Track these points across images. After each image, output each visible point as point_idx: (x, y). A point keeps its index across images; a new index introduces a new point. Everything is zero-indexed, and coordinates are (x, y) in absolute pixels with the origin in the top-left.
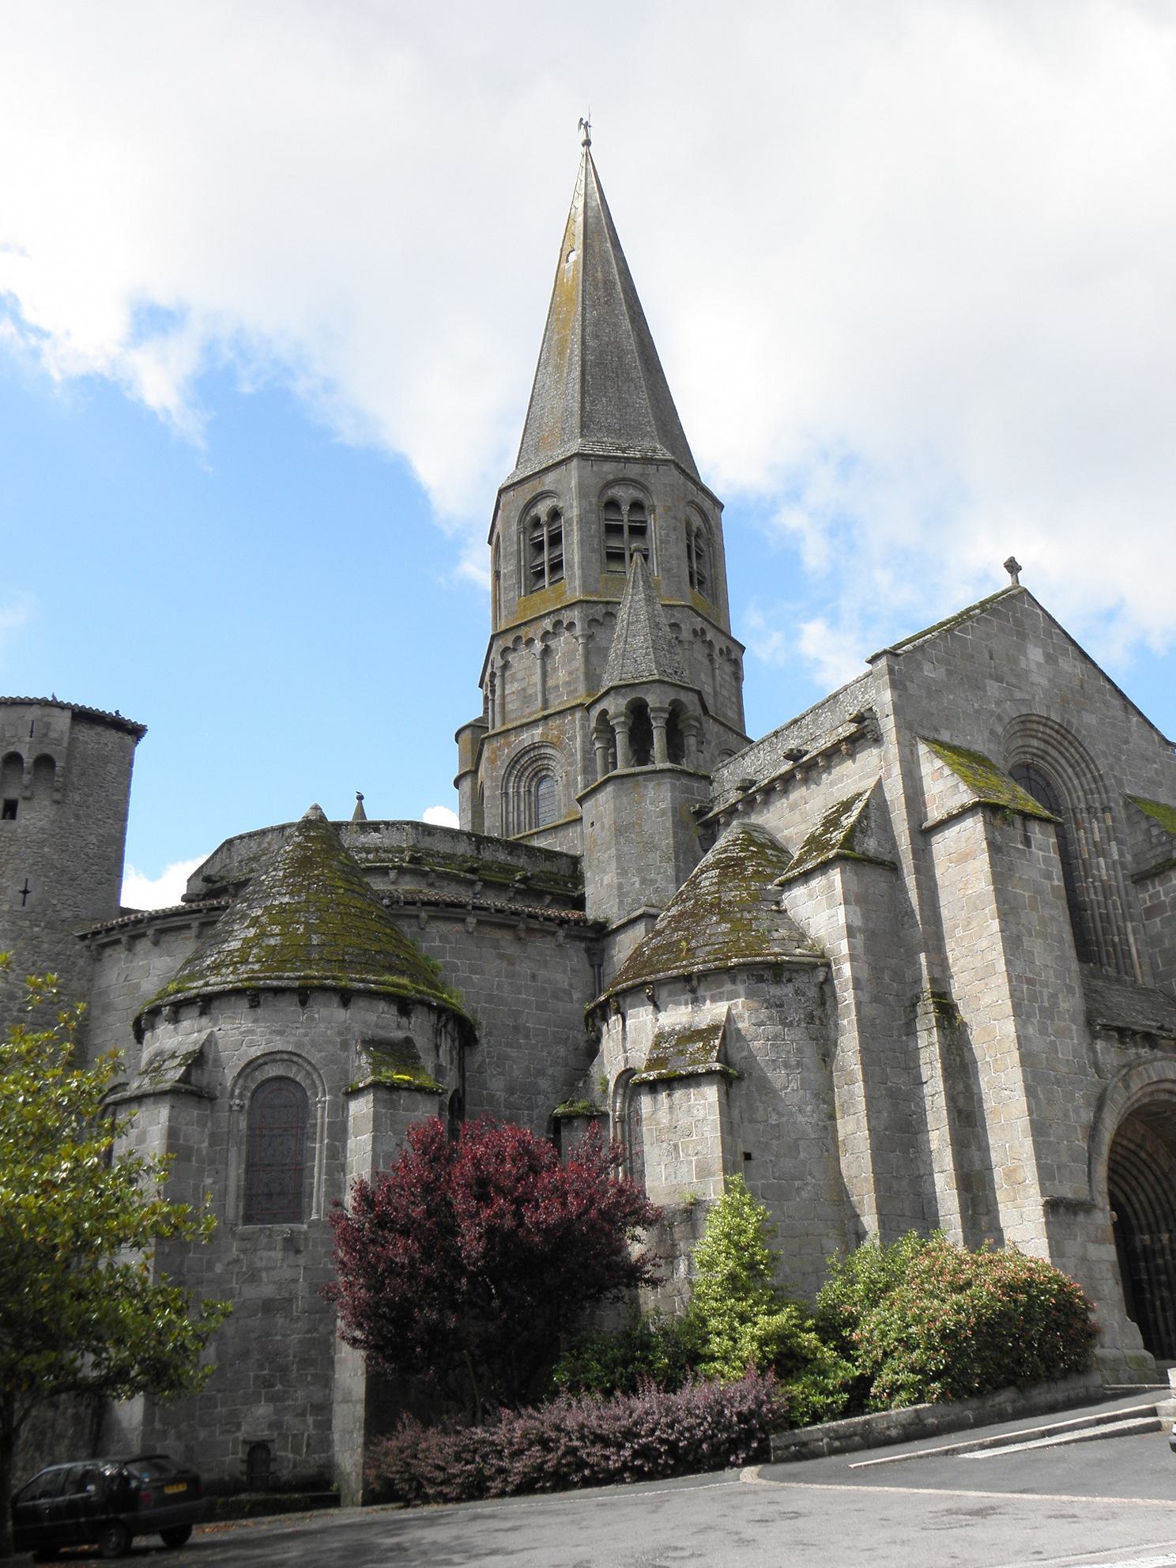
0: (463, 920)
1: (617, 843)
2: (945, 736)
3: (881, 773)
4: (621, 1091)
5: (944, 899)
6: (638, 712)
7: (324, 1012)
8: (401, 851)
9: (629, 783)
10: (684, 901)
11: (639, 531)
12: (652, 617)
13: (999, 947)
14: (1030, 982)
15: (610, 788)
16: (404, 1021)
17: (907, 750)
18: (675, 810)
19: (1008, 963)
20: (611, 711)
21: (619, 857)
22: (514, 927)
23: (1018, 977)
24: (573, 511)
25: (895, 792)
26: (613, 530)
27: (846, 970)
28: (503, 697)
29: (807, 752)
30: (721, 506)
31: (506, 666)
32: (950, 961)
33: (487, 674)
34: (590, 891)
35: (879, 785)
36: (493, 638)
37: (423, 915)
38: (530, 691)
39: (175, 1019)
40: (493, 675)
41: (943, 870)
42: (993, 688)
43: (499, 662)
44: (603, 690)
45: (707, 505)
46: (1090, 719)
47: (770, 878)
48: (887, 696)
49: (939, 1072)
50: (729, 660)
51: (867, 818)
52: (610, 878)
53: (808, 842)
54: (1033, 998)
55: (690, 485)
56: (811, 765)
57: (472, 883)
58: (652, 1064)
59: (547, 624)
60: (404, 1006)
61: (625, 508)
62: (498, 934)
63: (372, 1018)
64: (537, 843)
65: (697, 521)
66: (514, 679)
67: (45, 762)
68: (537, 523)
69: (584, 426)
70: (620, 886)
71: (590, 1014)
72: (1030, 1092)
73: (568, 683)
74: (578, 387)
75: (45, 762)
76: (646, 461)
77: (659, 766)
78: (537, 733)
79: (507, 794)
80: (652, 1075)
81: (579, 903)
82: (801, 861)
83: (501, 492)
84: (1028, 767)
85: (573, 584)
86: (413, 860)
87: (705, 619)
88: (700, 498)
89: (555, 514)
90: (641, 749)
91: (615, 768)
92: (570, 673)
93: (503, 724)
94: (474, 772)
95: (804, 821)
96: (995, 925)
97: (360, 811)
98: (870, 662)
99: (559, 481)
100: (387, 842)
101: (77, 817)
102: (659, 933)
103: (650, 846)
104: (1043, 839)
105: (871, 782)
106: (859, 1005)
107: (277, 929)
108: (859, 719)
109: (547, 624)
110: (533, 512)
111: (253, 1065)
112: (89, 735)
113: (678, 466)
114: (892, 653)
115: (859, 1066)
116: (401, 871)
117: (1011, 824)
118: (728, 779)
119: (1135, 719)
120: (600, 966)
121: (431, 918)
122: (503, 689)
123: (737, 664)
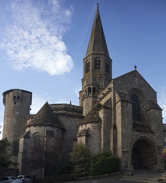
0: (65, 116)
7: (42, 127)
8: (63, 107)
9: (87, 98)
11: (99, 64)
12: (93, 76)
14: (125, 124)
16: (53, 129)
18: (92, 102)
19: (121, 121)
22: (72, 117)
23: (123, 123)
24: (91, 62)
26: (96, 64)
27: (103, 122)
30: (111, 60)
35: (111, 98)
41: (117, 109)
42: (129, 84)
45: (109, 61)
54: (125, 126)
55: (107, 58)
57: (72, 111)
59: (87, 77)
61: (98, 61)
62: (70, 118)
63: (48, 128)
69: (93, 50)
72: (122, 138)
76: (101, 54)
83: (83, 60)
88: (109, 60)
89: (89, 63)
96: (121, 116)
97: (71, 103)
100: (62, 106)
101: (23, 104)
103: (89, 106)
106: (104, 127)
109: (87, 77)
111: (34, 134)
113: (105, 55)
117: (125, 103)
119: (151, 89)
121: (61, 116)
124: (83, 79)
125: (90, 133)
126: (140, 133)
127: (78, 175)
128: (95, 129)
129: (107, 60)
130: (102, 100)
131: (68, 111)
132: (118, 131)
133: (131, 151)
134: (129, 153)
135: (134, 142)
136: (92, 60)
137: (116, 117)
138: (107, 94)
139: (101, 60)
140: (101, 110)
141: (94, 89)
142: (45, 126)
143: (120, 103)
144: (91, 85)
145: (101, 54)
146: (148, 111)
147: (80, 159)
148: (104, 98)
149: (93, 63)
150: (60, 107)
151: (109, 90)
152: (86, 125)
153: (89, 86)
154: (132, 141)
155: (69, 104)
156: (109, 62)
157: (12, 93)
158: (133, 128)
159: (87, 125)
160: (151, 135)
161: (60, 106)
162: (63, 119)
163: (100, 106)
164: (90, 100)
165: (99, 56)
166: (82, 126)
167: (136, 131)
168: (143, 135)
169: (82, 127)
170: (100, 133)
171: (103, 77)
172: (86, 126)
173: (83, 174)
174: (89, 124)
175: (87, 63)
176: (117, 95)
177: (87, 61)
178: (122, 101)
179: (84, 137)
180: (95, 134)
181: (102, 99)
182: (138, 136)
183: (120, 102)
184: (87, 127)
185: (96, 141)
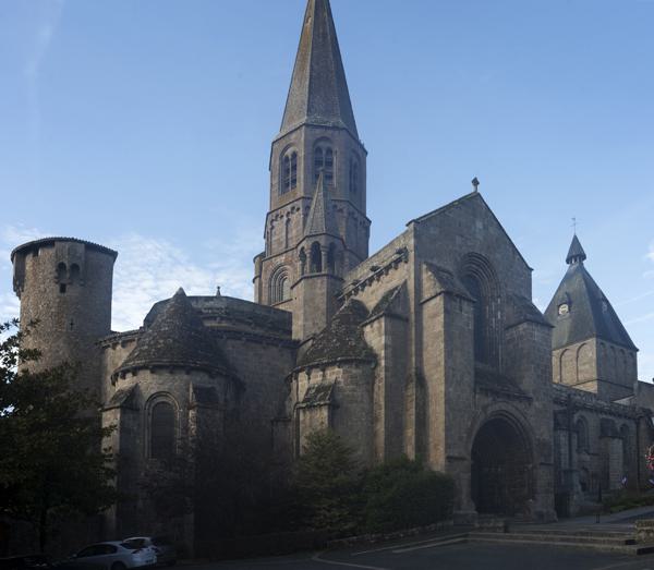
0: (240, 339)
2: (435, 262)
5: (425, 334)
6: (316, 246)
9: (310, 281)
11: (330, 164)
12: (325, 204)
13: (443, 355)
14: (453, 369)
22: (261, 343)
24: (301, 154)
26: (318, 163)
27: (383, 363)
31: (272, 228)
34: (294, 328)
35: (405, 282)
39: (124, 377)
41: (426, 322)
42: (458, 240)
45: (360, 152)
46: (498, 256)
47: (358, 324)
52: (301, 322)
54: (454, 376)
57: (250, 324)
58: (305, 401)
59: (289, 208)
61: (324, 152)
62: (253, 345)
65: (355, 160)
67: (75, 267)
71: (286, 379)
72: (447, 414)
75: (75, 267)
76: (335, 128)
77: (323, 272)
80: (304, 405)
81: (290, 332)
83: (274, 143)
84: (470, 276)
89: (295, 155)
96: (442, 346)
99: (296, 139)
104: (468, 309)
106: (386, 377)
107: (161, 341)
108: (399, 252)
109: (289, 208)
112: (93, 255)
117: (455, 301)
123: (367, 230)
124: (274, 214)
125: (339, 397)
126: (494, 400)
127: (329, 530)
129: (354, 151)
130: (363, 290)
131: (238, 320)
132: (430, 391)
133: (469, 457)
134: (466, 463)
135: (477, 427)
136: (305, 146)
137: (425, 345)
138: (388, 268)
139: (335, 149)
140: (376, 324)
141: (332, 247)
143: (439, 301)
145: (335, 128)
146: (509, 327)
147: (335, 480)
148: (375, 283)
151: (398, 256)
152: (323, 370)
153: (317, 239)
154: (472, 426)
156: (358, 156)
157: (51, 251)
158: (476, 382)
159: (328, 372)
160: (521, 406)
162: (231, 348)
163: (360, 314)
164: (321, 287)
165: (328, 133)
166: (309, 374)
167: (486, 392)
168: (501, 406)
169: (309, 379)
170: (372, 398)
171: (341, 210)
172: (324, 376)
173: (346, 527)
174: (337, 369)
175: (287, 157)
176: (426, 275)
177: (285, 149)
178: (448, 295)
179: (325, 412)
180: (356, 402)
181: (364, 285)
182: (490, 410)
183: (438, 298)
184: (328, 377)
185: (359, 423)
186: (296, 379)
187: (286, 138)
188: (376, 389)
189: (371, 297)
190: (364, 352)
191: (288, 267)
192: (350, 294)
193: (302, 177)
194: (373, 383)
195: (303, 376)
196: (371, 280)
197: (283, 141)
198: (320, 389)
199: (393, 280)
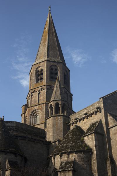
0: (25, 140)
1: (53, 128)
2: (112, 113)
3: (101, 118)
4: (53, 172)
6: (57, 105)
8: (13, 127)
9: (55, 117)
10: (66, 139)
15: (52, 118)
17: (106, 114)
18: (63, 122)
20: (53, 104)
21: (53, 130)
25: (104, 122)
28: (31, 101)
29: (88, 114)
30: (70, 71)
31: (32, 95)
32: (113, 152)
33: (28, 96)
35: (101, 120)
36: (30, 90)
37: (19, 139)
38: (36, 100)
40: (29, 97)
43: (31, 95)
44: (51, 101)
45: (67, 70)
48: (102, 105)
49: (111, 171)
50: (70, 97)
51: (99, 126)
53: (88, 130)
56: (89, 116)
57: (26, 133)
59: (40, 88)
60: (15, 154)
61: (54, 70)
64: (36, 126)
65: (66, 73)
66: (33, 98)
68: (39, 71)
70: (53, 135)
73: (43, 99)
74: (47, 49)
77: (61, 115)
78: (37, 107)
79: (31, 118)
82: (87, 133)
85: (45, 82)
86: (16, 128)
87: (67, 90)
89: (42, 70)
90: (57, 111)
91: (53, 114)
92: (43, 97)
93: (31, 105)
94: (25, 113)
95: (87, 126)
98: (99, 99)
99: (43, 64)
102: (61, 144)
105: (100, 119)
108: (97, 109)
110: (38, 69)
114: (103, 98)
115: (97, 170)
116: (14, 130)
118: (73, 118)
120: (49, 149)
121: (20, 139)
122: (31, 99)
128: (84, 161)
130: (80, 122)
136: (47, 67)
138: (92, 114)
140: (90, 136)
142: (6, 154)
144: (61, 101)
148: (85, 120)
149: (49, 71)
150: (9, 126)
151: (97, 110)
152: (68, 155)
153: (58, 102)
155: (23, 122)
156: (67, 73)
159: (70, 156)
161: (9, 124)
163: (79, 132)
164: (60, 120)
165: (56, 64)
166: (61, 156)
169: (61, 158)
170: (91, 168)
172: (68, 157)
174: (74, 154)
176: (110, 118)
180: (84, 169)
181: (80, 120)
184: (70, 158)
186: (54, 158)
187: (39, 64)
188: (92, 163)
189: (85, 125)
190: (86, 148)
191: (39, 110)
192: (73, 123)
193: (45, 78)
194: (91, 161)
195: (58, 157)
196: (84, 118)
197: (37, 65)
198: (67, 163)
199: (95, 119)
